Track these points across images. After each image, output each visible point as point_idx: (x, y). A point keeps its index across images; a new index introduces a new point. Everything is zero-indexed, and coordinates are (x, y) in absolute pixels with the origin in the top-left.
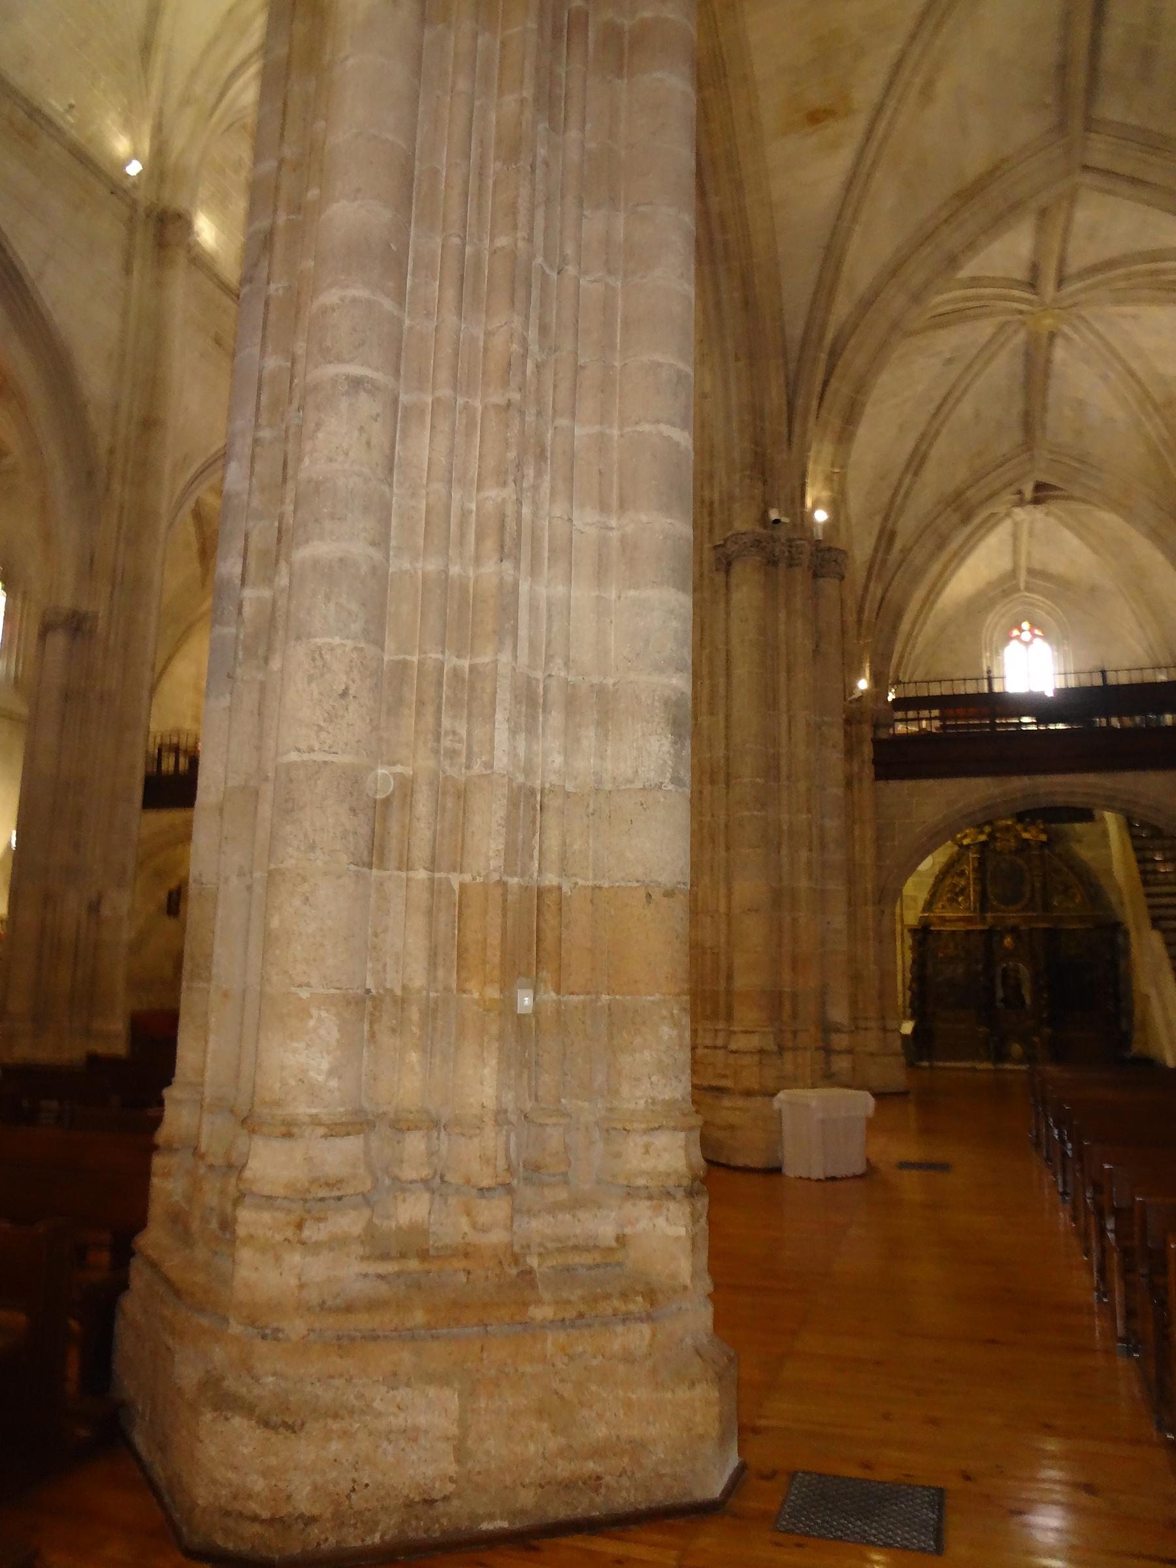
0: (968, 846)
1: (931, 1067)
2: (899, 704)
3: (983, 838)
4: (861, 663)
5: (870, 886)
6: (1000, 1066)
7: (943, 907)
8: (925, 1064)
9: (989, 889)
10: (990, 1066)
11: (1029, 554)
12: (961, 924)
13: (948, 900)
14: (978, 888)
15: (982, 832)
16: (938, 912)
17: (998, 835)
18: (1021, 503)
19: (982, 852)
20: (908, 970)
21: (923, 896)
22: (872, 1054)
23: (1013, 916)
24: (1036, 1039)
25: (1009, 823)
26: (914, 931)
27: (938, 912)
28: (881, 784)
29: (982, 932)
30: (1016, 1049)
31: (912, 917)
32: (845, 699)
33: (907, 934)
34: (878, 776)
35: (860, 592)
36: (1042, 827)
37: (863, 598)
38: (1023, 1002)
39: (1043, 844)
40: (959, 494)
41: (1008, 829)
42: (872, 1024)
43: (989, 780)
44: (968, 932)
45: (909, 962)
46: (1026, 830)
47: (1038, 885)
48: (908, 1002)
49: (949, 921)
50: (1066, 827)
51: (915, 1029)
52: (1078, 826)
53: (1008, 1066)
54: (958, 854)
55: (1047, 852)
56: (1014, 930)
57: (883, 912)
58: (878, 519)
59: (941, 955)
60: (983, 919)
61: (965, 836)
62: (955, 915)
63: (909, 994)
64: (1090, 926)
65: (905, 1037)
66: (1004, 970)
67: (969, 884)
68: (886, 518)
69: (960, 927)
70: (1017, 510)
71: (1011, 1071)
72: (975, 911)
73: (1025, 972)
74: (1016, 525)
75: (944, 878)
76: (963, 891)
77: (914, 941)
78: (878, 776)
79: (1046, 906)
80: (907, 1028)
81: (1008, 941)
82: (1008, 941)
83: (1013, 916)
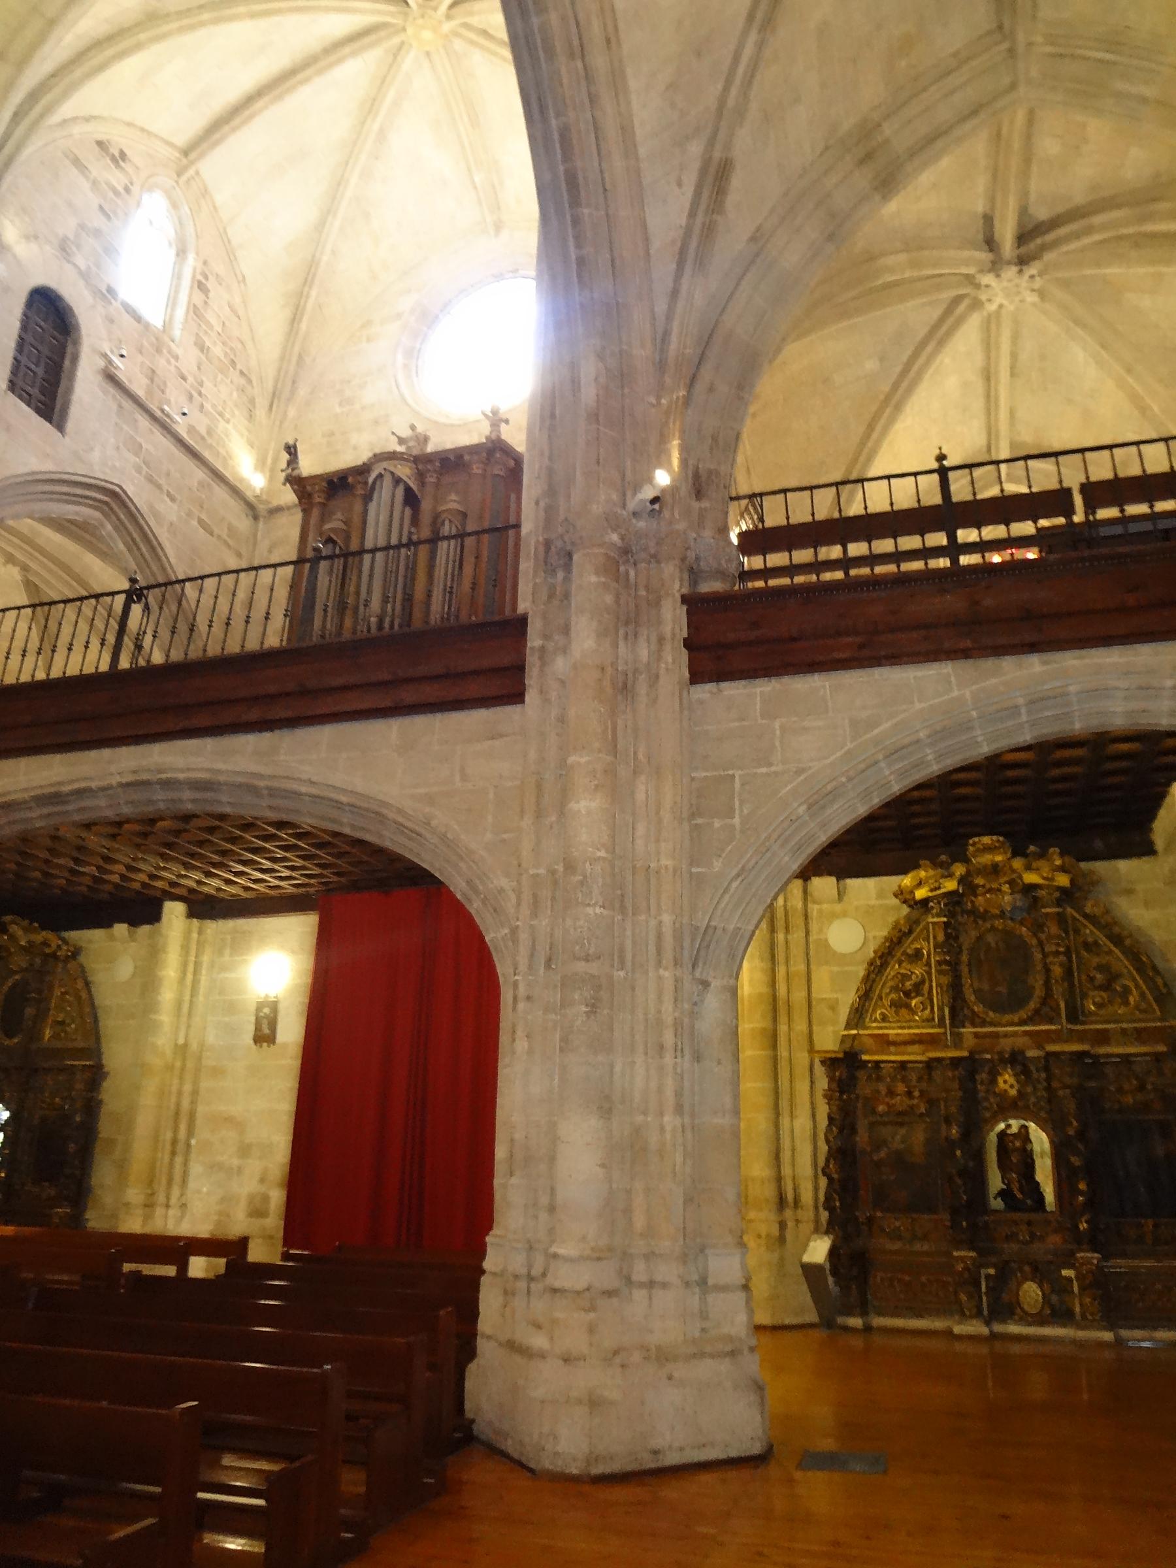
0: (925, 902)
1: (868, 1329)
2: (754, 541)
3: (950, 885)
4: (663, 439)
5: (667, 918)
6: (998, 1328)
7: (884, 1018)
8: (856, 1322)
9: (967, 981)
10: (975, 1327)
11: (1012, 413)
12: (916, 1048)
13: (893, 1004)
14: (945, 980)
15: (950, 876)
16: (874, 1028)
17: (980, 881)
18: (995, 267)
19: (952, 915)
20: (821, 1136)
21: (848, 998)
22: (662, 1356)
23: (1013, 1032)
24: (1065, 1273)
25: (999, 858)
26: (831, 1063)
27: (874, 1028)
28: (704, 691)
29: (955, 1062)
30: (1031, 1293)
31: (829, 1039)
32: (624, 506)
33: (820, 1070)
34: (697, 677)
35: (661, 307)
36: (1058, 862)
37: (669, 317)
38: (1040, 1198)
39: (1066, 896)
40: (867, 130)
41: (995, 870)
42: (668, 1271)
43: (946, 669)
44: (930, 1065)
45: (823, 1123)
46: (1028, 868)
47: (1057, 971)
48: (822, 1198)
49: (894, 1043)
50: (1100, 867)
51: (833, 1253)
52: (1124, 866)
53: (1014, 1329)
54: (908, 917)
55: (1069, 910)
56: (1015, 1059)
57: (705, 984)
58: (696, 149)
59: (881, 1108)
60: (958, 1041)
61: (920, 884)
62: (905, 1034)
63: (823, 1182)
64: (1161, 1048)
65: (810, 1271)
66: (1002, 1135)
67: (929, 973)
68: (711, 142)
69: (915, 1055)
70: (988, 279)
71: (1018, 1338)
72: (942, 1023)
73: (1040, 1139)
74: (989, 327)
75: (884, 965)
76: (917, 988)
77: (831, 1079)
78: (697, 677)
80: (818, 1250)
81: (1007, 1082)
83: (1013, 1032)
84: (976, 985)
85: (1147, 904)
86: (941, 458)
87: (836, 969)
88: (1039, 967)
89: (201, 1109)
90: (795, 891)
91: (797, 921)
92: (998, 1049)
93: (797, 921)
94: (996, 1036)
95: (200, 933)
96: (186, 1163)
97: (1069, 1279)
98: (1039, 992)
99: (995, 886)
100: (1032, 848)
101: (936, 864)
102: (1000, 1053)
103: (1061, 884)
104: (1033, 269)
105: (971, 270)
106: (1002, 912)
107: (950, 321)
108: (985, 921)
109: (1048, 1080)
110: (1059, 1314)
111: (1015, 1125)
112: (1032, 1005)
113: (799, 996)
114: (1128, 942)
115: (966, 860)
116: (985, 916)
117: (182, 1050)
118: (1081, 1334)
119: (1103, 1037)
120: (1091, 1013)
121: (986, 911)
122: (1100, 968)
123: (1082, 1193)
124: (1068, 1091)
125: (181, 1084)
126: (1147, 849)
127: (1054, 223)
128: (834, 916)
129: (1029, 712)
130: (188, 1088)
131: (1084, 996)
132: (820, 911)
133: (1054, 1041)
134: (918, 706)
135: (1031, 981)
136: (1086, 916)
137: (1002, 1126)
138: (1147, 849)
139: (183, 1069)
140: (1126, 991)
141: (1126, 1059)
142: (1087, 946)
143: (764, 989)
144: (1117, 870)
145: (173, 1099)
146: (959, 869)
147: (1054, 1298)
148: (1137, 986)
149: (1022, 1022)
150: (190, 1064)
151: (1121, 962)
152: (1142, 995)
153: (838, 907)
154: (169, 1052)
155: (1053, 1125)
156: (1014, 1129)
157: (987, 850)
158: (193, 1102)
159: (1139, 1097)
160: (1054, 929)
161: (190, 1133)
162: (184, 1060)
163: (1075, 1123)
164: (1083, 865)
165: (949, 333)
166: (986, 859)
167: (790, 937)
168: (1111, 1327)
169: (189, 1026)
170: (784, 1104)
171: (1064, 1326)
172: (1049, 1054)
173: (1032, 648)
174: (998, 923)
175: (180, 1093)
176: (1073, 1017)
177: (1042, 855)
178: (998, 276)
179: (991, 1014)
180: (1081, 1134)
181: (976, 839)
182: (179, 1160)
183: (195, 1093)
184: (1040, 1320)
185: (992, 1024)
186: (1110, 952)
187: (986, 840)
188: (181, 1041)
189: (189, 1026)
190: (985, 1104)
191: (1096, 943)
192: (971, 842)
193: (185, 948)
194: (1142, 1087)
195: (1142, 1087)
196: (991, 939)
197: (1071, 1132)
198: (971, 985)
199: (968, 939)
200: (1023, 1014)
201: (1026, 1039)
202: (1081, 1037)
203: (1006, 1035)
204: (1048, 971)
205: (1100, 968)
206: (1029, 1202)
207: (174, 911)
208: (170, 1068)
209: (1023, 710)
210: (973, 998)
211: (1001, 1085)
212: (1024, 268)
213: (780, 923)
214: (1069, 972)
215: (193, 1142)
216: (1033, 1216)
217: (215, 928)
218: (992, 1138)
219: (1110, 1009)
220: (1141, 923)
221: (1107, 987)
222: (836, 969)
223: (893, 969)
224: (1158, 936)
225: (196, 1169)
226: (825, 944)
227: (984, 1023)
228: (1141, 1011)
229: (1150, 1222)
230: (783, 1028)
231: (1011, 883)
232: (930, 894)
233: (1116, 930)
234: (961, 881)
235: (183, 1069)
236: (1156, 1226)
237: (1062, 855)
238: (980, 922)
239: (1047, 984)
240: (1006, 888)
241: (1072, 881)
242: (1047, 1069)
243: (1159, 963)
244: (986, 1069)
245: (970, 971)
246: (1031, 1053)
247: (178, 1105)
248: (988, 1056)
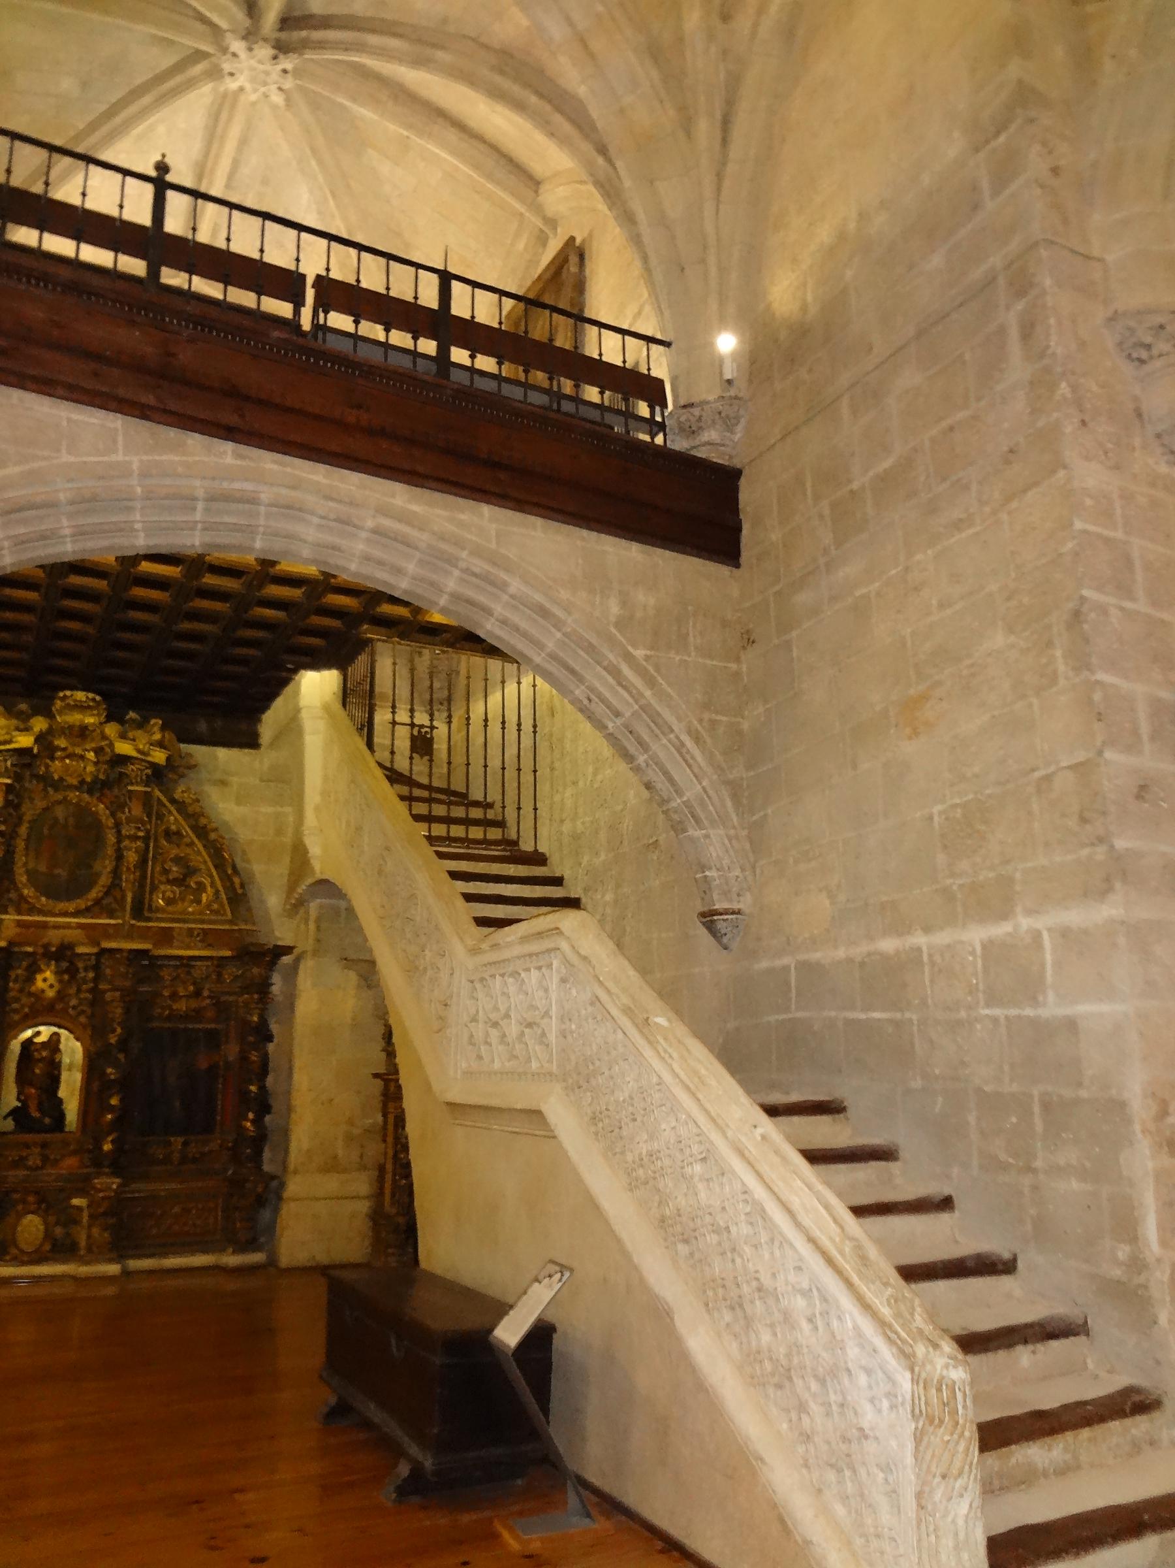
3: (25, 741)
15: (27, 729)
17: (61, 742)
18: (250, 36)
19: (18, 778)
23: (65, 923)
25: (90, 720)
36: (157, 736)
38: (61, 1116)
39: (157, 774)
41: (83, 732)
46: (123, 736)
47: (132, 857)
50: (199, 751)
52: (222, 753)
55: (157, 793)
56: (63, 955)
66: (29, 1042)
70: (237, 46)
79: (139, 910)
81: (46, 980)
82: (46, 980)
83: (65, 923)
84: (31, 865)
85: (239, 801)
86: (162, 168)
88: (110, 851)
92: (45, 940)
94: (45, 926)
97: (79, 1209)
98: (104, 880)
99: (78, 751)
100: (132, 715)
102: (46, 946)
103: (157, 761)
104: (288, 63)
105: (223, 24)
106: (82, 782)
107: (178, 79)
109: (96, 980)
110: (61, 1249)
111: (45, 1032)
112: (94, 894)
114: (213, 836)
115: (49, 715)
116: (58, 785)
118: (84, 1270)
119: (166, 937)
120: (159, 909)
121: (61, 779)
122: (177, 860)
123: (111, 1109)
124: (118, 994)
126: (251, 742)
127: (326, 22)
129: (207, 510)
131: (154, 888)
133: (109, 937)
134: (66, 458)
135: (97, 867)
136: (173, 801)
137: (29, 1033)
138: (251, 742)
140: (201, 887)
141: (187, 963)
142: (168, 834)
144: (216, 758)
146: (39, 724)
147: (59, 1231)
148: (213, 884)
149: (77, 913)
151: (200, 856)
152: (217, 892)
155: (93, 1032)
156: (43, 1038)
157: (79, 708)
159: (194, 1004)
160: (137, 810)
163: (119, 1030)
164: (182, 746)
165: (176, 92)
166: (75, 718)
168: (120, 1258)
171: (64, 1261)
172: (104, 951)
173: (229, 433)
174: (73, 796)
176: (139, 910)
177: (141, 725)
178: (250, 49)
180: (123, 1044)
181: (68, 693)
184: (38, 1258)
185: (41, 912)
186: (192, 844)
187: (80, 695)
190: (15, 1006)
191: (178, 833)
192: (61, 694)
194: (197, 994)
195: (197, 994)
196: (60, 812)
197: (113, 1041)
198: (25, 864)
199: (29, 811)
200: (81, 903)
201: (79, 931)
202: (144, 934)
203: (57, 927)
204: (119, 857)
205: (177, 860)
206: (47, 1120)
209: (200, 505)
210: (24, 879)
211: (40, 984)
212: (281, 56)
214: (143, 861)
216: (58, 1136)
218: (15, 1046)
219: (180, 906)
220: (227, 817)
221: (180, 882)
224: (243, 834)
227: (32, 910)
228: (216, 912)
229: (181, 1140)
231: (98, 751)
233: (203, 821)
234: (39, 739)
236: (185, 1144)
237: (163, 728)
239: (116, 873)
240: (91, 755)
241: (168, 759)
242: (96, 968)
243: (238, 861)
244: (24, 964)
245: (27, 848)
246: (80, 950)
248: (30, 949)
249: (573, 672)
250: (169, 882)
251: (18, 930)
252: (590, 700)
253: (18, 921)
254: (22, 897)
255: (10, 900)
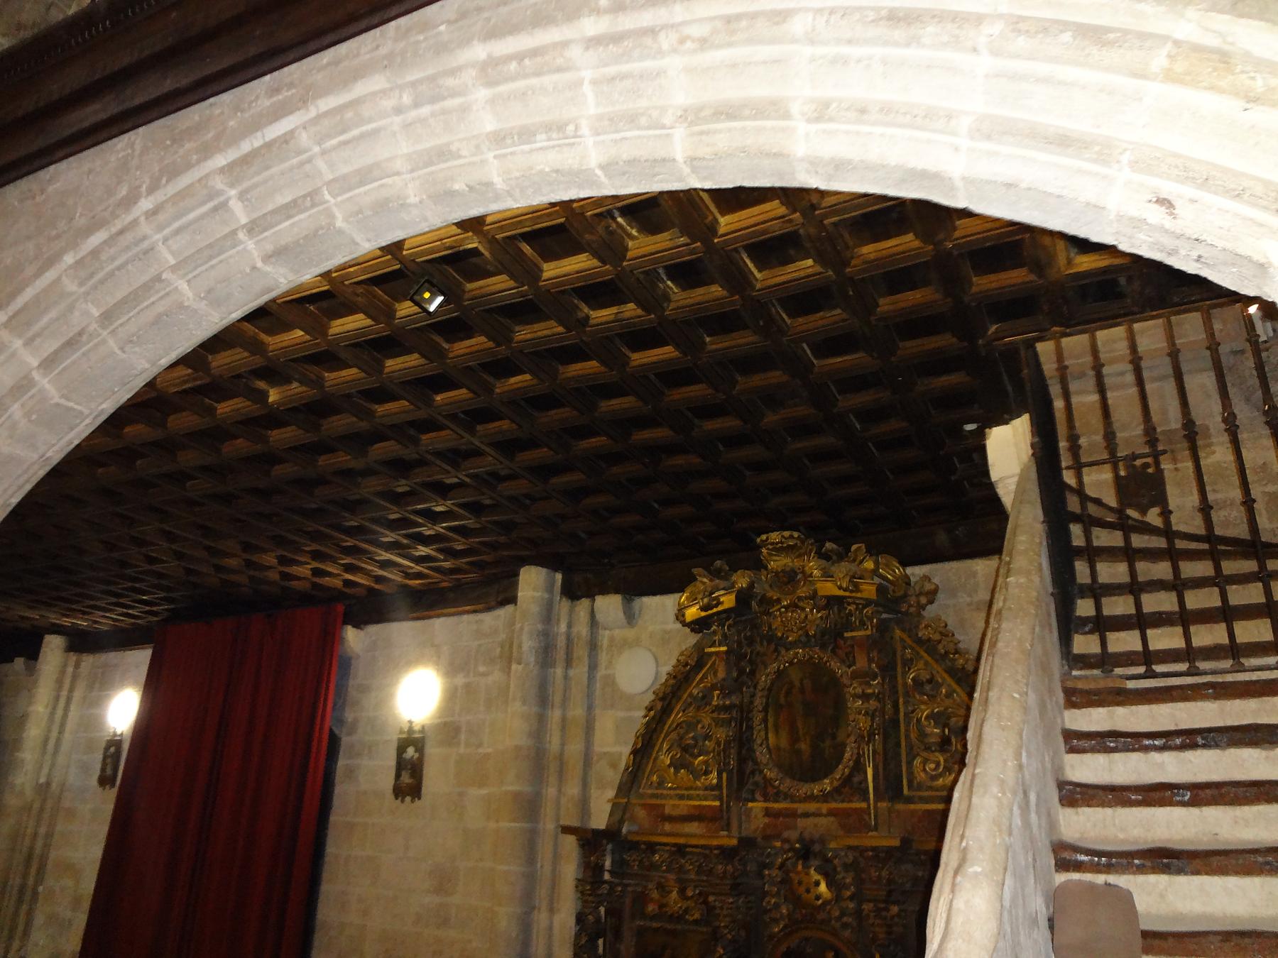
15: (728, 589)
41: (789, 579)
46: (827, 575)
87: (621, 714)
89: (53, 855)
90: (582, 614)
91: (581, 652)
93: (581, 652)
94: (793, 814)
95: (77, 666)
96: (30, 914)
101: (716, 574)
108: (787, 650)
113: (575, 748)
115: (759, 565)
117: (43, 790)
125: (38, 825)
128: (625, 644)
130: (42, 830)
132: (612, 639)
139: (42, 810)
143: (523, 741)
145: (27, 841)
146: (742, 580)
149: (825, 797)
150: (49, 804)
153: (630, 633)
154: (29, 792)
157: (779, 549)
158: (47, 846)
161: (40, 878)
162: (44, 800)
166: (778, 563)
167: (571, 673)
169: (53, 765)
170: (542, 892)
175: (35, 835)
179: (788, 782)
181: (764, 537)
182: (25, 907)
183: (49, 835)
188: (42, 780)
189: (53, 765)
193: (60, 682)
196: (795, 675)
200: (827, 785)
201: (832, 819)
203: (806, 815)
207: (53, 646)
208: (28, 808)
213: (560, 655)
215: (41, 889)
217: (88, 661)
222: (621, 714)
223: (677, 716)
225: (39, 919)
226: (610, 681)
227: (778, 796)
230: (551, 791)
232: (703, 614)
235: (42, 810)
238: (783, 652)
247: (31, 848)
249: (1063, 142)
250: (928, 748)
251: (766, 820)
252: (1165, 202)
253: (767, 809)
254: (768, 782)
255: (756, 784)
